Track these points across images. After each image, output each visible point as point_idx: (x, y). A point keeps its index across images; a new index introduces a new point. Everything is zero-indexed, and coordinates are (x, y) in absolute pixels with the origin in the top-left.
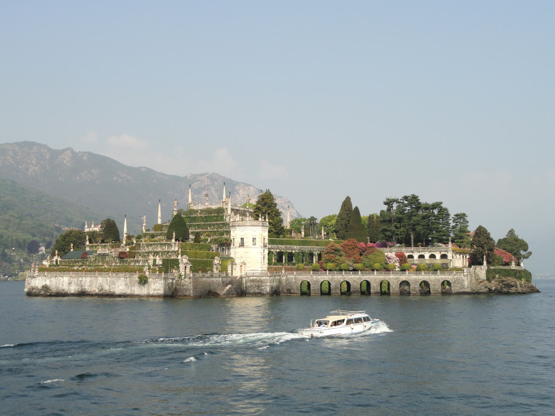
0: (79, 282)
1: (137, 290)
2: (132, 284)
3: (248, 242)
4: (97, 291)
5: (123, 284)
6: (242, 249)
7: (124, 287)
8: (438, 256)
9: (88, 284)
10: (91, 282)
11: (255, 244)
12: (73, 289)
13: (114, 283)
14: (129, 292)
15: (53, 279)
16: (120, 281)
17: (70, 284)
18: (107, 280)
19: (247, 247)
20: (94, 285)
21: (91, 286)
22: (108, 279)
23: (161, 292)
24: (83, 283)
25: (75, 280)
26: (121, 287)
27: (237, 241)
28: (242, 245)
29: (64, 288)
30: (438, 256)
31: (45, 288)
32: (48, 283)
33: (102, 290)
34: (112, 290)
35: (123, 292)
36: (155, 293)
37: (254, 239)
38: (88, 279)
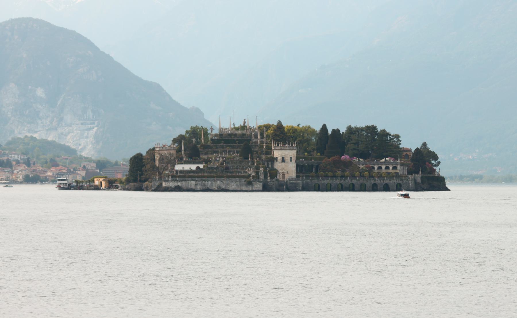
3: (287, 159)
4: (216, 189)
6: (283, 164)
8: (391, 168)
11: (291, 161)
13: (228, 184)
14: (239, 189)
17: (196, 185)
19: (287, 163)
20: (214, 186)
21: (212, 185)
22: (224, 182)
25: (200, 182)
26: (233, 187)
27: (280, 159)
28: (283, 160)
30: (391, 168)
32: (179, 184)
37: (291, 158)
38: (210, 183)
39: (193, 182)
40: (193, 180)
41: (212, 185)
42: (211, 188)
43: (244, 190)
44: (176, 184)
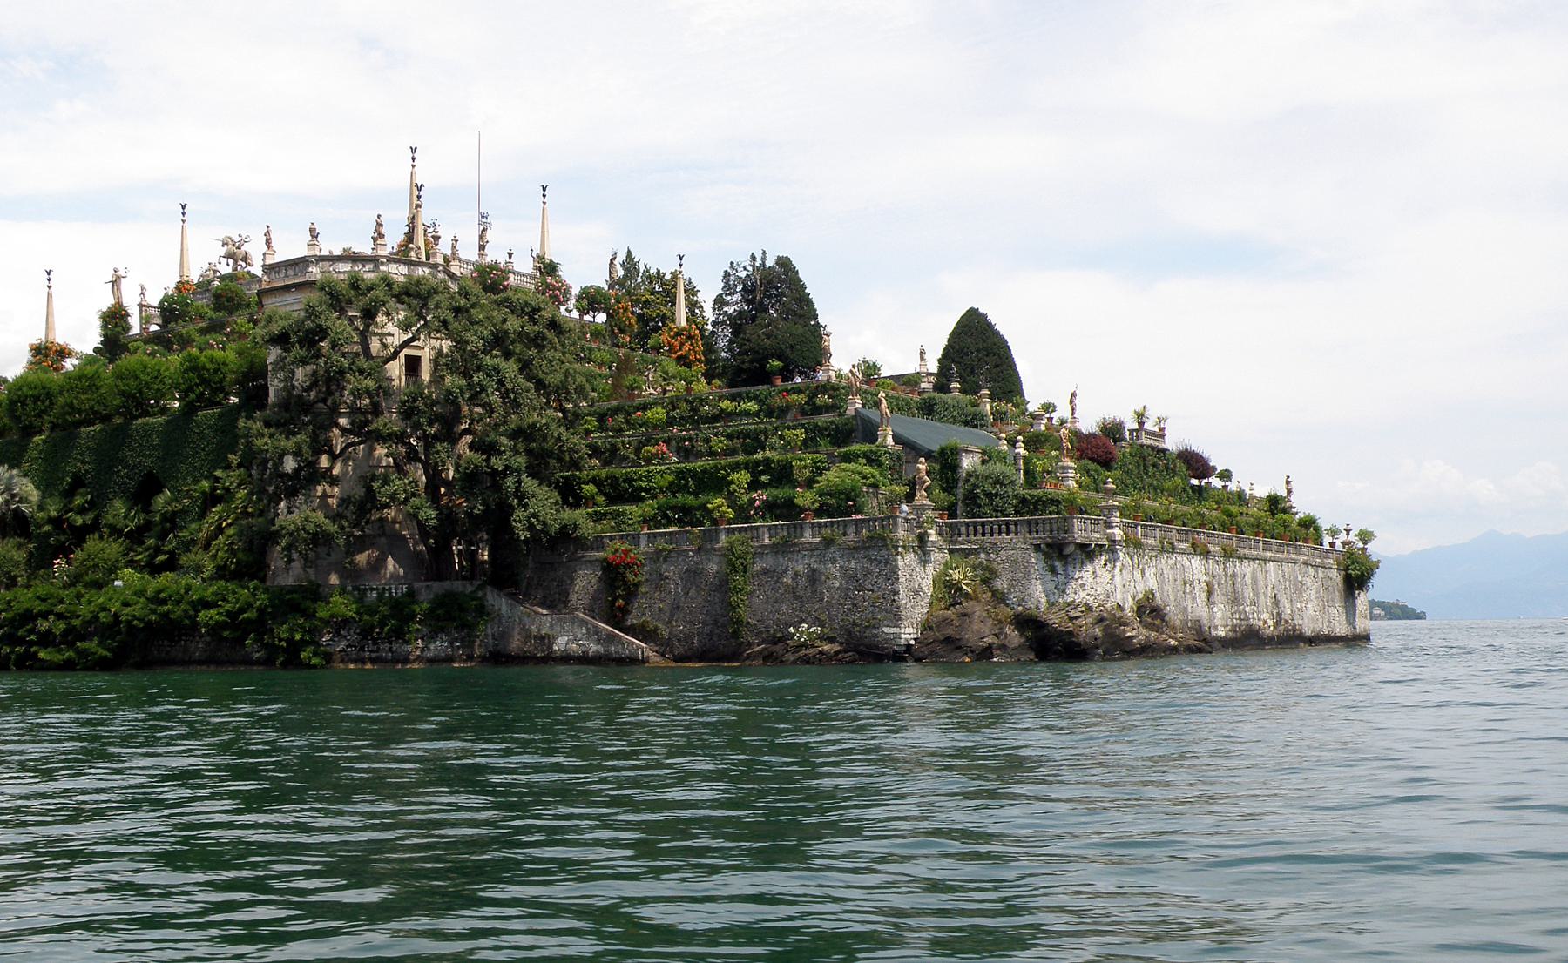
31: (1149, 610)
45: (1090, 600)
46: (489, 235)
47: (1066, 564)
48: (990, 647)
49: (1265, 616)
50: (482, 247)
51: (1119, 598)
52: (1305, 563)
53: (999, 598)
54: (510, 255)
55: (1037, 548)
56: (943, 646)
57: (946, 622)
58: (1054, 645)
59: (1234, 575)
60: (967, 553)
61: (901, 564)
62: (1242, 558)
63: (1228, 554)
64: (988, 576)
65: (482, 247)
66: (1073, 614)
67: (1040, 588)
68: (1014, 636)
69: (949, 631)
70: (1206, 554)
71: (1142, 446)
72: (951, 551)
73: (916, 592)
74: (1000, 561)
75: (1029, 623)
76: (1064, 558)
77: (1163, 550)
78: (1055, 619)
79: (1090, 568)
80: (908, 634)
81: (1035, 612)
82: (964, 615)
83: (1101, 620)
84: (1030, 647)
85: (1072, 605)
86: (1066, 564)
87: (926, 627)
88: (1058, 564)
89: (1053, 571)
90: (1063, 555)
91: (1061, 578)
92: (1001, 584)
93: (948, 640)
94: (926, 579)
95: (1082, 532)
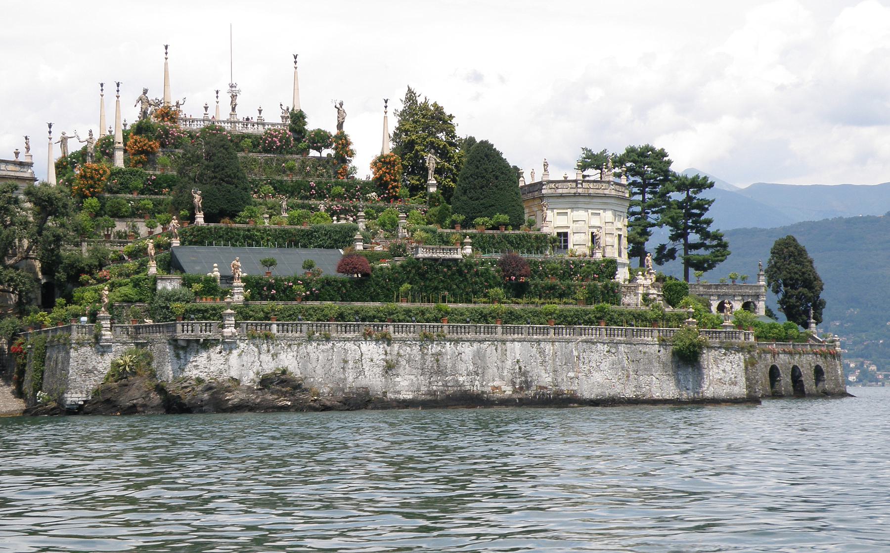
0: (429, 359)
1: (662, 386)
2: (641, 365)
4: (508, 391)
5: (605, 365)
7: (609, 374)
9: (466, 364)
10: (479, 356)
12: (406, 384)
14: (629, 392)
15: (316, 351)
16: (595, 356)
17: (390, 368)
18: (542, 352)
20: (492, 371)
21: (479, 370)
22: (548, 348)
23: (740, 390)
24: (447, 361)
26: (598, 377)
29: (363, 382)
32: (288, 360)
33: (527, 384)
34: (564, 388)
35: (608, 393)
36: (723, 391)
38: (468, 350)
39: (372, 351)
40: (367, 336)
41: (479, 370)
42: (477, 388)
43: (657, 395)
44: (269, 366)
45: (203, 376)
46: (238, 100)
47: (186, 353)
48: (134, 406)
49: (497, 383)
50: (233, 109)
51: (234, 374)
52: (586, 342)
53: (153, 375)
54: (260, 111)
55: (170, 344)
56: (103, 404)
57: (109, 390)
58: (174, 405)
59: (439, 354)
60: (143, 345)
61: (73, 353)
62: (457, 341)
63: (427, 338)
64: (149, 358)
65: (233, 109)
66: (185, 385)
67: (170, 368)
68: (156, 398)
69: (108, 396)
70: (386, 339)
71: (418, 259)
72: (137, 344)
73: (89, 372)
74: (154, 350)
75: (160, 389)
76: (183, 348)
77: (310, 339)
78: (171, 389)
79: (205, 354)
80: (74, 397)
81: (164, 384)
82: (126, 385)
83: (209, 388)
84: (164, 406)
85: (185, 379)
86: (186, 353)
87: (96, 393)
88: (181, 352)
89: (178, 356)
90: (184, 349)
91: (183, 361)
92: (154, 365)
93: (108, 401)
94: (104, 364)
95: (183, 333)
